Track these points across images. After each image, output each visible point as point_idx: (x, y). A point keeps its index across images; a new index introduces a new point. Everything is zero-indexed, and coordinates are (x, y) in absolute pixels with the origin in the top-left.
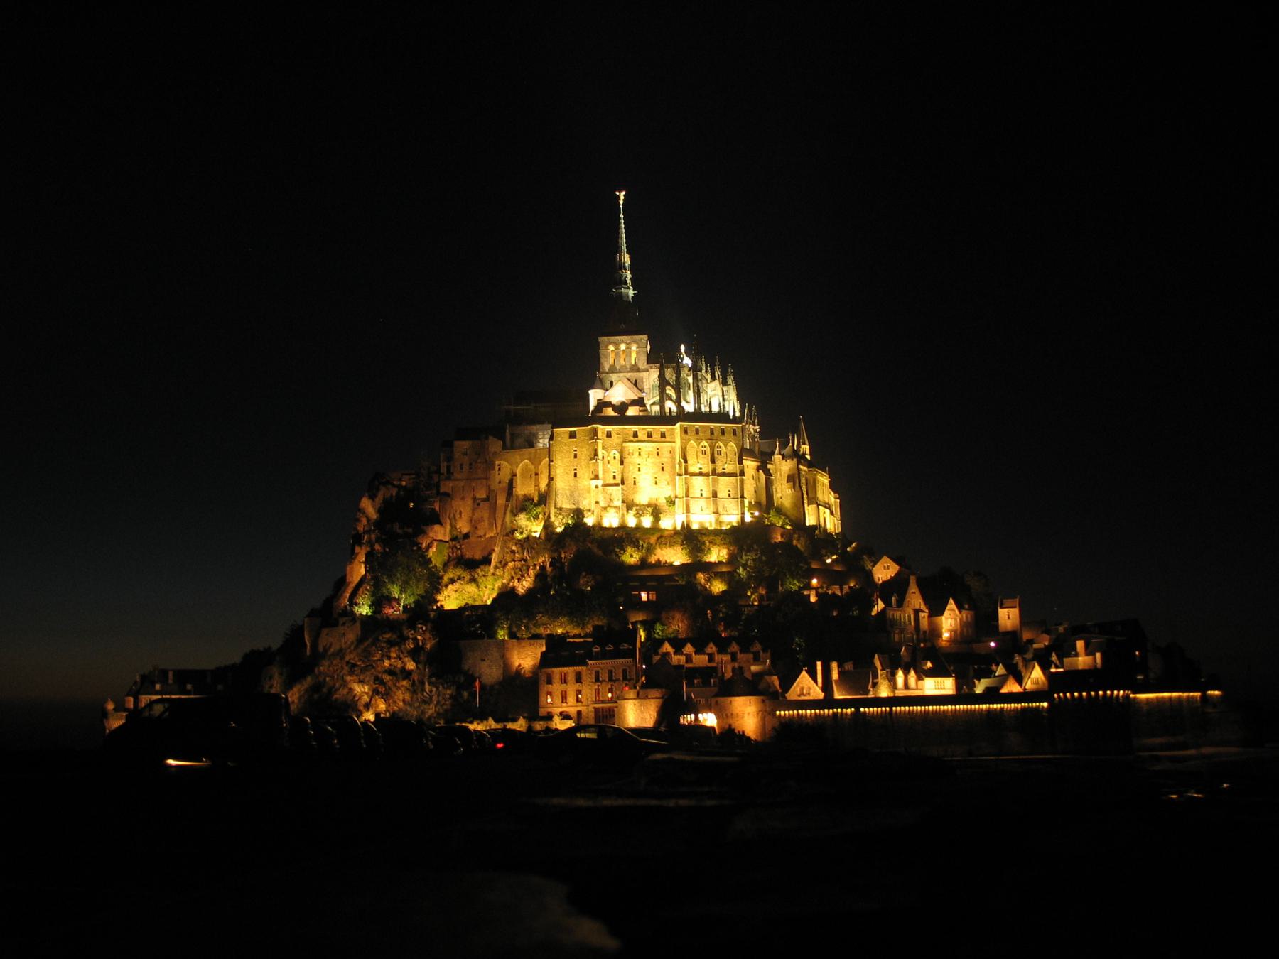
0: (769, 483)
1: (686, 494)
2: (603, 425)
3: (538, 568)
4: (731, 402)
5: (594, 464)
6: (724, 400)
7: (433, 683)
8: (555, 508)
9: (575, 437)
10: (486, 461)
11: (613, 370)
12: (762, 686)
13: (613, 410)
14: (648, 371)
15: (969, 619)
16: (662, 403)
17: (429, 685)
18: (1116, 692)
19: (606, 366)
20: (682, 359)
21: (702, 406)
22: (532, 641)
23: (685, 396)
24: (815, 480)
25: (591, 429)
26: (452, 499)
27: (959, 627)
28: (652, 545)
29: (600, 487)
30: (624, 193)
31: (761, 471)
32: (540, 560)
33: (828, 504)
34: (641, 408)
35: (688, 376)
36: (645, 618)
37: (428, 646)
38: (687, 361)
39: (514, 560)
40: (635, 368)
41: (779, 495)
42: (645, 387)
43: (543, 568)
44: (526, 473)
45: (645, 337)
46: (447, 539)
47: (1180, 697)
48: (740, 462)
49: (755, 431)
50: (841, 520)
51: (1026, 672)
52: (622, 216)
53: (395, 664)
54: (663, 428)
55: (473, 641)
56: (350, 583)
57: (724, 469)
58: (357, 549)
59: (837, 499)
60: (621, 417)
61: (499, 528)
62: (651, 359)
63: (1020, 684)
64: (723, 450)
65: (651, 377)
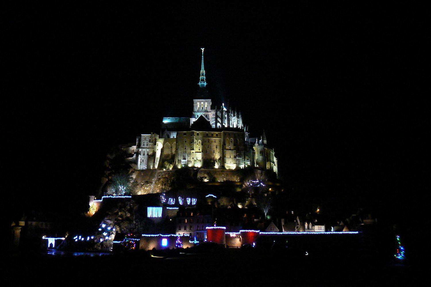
4: (240, 124)
6: (238, 123)
14: (211, 112)
16: (216, 124)
20: (223, 108)
21: (230, 125)
24: (270, 153)
30: (204, 49)
35: (225, 114)
38: (225, 109)
43: (173, 181)
45: (210, 100)
52: (203, 57)
54: (217, 133)
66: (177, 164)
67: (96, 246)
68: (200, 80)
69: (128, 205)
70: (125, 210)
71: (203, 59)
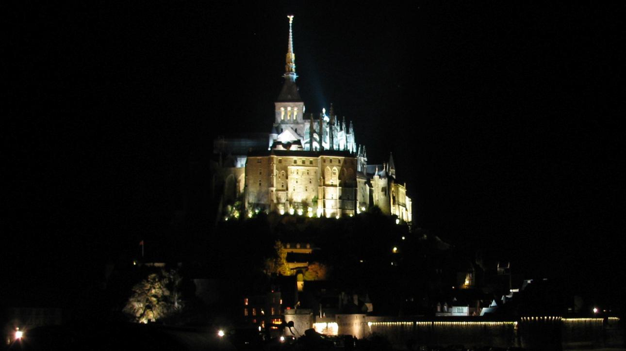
0: (371, 192)
4: (351, 143)
6: (347, 142)
12: (363, 309)
13: (283, 146)
14: (301, 124)
16: (311, 143)
18: (554, 318)
20: (323, 117)
23: (324, 139)
30: (292, 17)
31: (367, 185)
34: (299, 146)
35: (327, 127)
37: (177, 282)
38: (326, 119)
40: (296, 121)
41: (377, 199)
49: (364, 160)
50: (412, 213)
52: (291, 31)
53: (158, 292)
54: (311, 159)
71: (291, 34)
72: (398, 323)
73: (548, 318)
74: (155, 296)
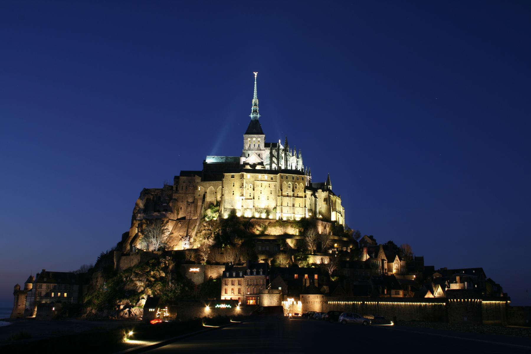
0: (316, 201)
1: (281, 204)
2: (246, 173)
3: (216, 233)
4: (301, 165)
5: (242, 190)
6: (297, 165)
7: (173, 283)
8: (224, 208)
9: (234, 177)
10: (194, 186)
11: (249, 149)
12: (322, 290)
15: (404, 265)
16: (271, 165)
17: (171, 283)
18: (476, 300)
19: (247, 147)
21: (288, 167)
22: (217, 266)
23: (280, 162)
25: (241, 174)
26: (178, 202)
27: (400, 267)
28: (266, 226)
29: (244, 199)
30: (257, 73)
31: (313, 196)
32: (217, 230)
33: (340, 212)
34: (262, 166)
35: (282, 153)
36: (265, 258)
37: (171, 267)
38: (282, 147)
39: (205, 230)
41: (320, 207)
42: (263, 157)
43: (218, 234)
44: (211, 191)
45: (264, 136)
46: (175, 219)
47: (499, 303)
48: (305, 192)
49: (310, 178)
51: (435, 289)
52: (255, 83)
53: (156, 273)
54: (272, 176)
55: (191, 265)
56: (130, 236)
57: (298, 194)
58: (135, 222)
59: (344, 209)
60: (253, 170)
61: (198, 215)
62: (267, 145)
63: (433, 294)
64: (298, 186)
65: (266, 153)
66: (223, 212)
67: (122, 314)
68: (252, 111)
69: (162, 262)
70: (159, 269)
71: (255, 85)
72: (350, 302)
73: (471, 300)
74: (154, 277)
